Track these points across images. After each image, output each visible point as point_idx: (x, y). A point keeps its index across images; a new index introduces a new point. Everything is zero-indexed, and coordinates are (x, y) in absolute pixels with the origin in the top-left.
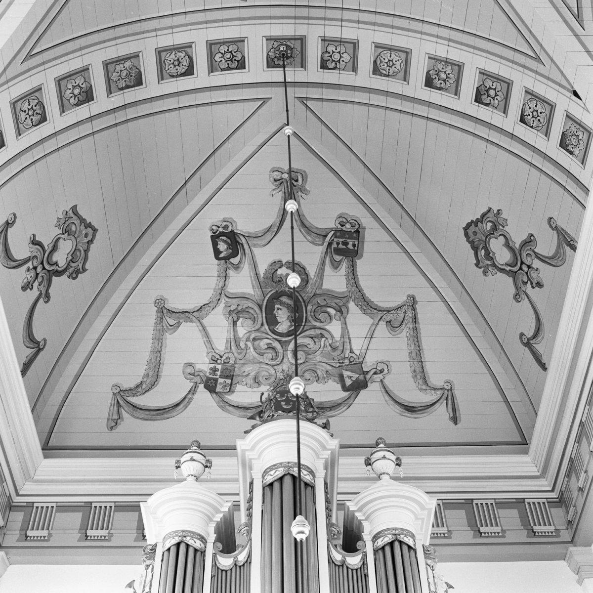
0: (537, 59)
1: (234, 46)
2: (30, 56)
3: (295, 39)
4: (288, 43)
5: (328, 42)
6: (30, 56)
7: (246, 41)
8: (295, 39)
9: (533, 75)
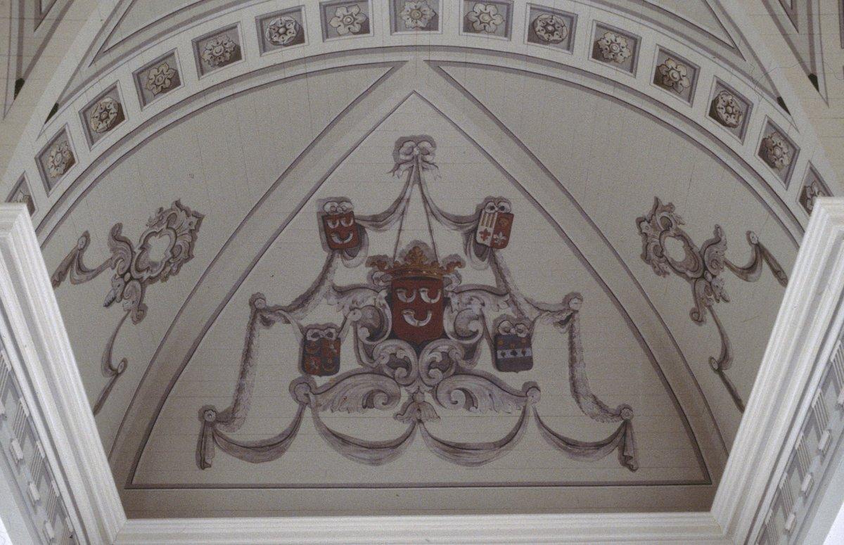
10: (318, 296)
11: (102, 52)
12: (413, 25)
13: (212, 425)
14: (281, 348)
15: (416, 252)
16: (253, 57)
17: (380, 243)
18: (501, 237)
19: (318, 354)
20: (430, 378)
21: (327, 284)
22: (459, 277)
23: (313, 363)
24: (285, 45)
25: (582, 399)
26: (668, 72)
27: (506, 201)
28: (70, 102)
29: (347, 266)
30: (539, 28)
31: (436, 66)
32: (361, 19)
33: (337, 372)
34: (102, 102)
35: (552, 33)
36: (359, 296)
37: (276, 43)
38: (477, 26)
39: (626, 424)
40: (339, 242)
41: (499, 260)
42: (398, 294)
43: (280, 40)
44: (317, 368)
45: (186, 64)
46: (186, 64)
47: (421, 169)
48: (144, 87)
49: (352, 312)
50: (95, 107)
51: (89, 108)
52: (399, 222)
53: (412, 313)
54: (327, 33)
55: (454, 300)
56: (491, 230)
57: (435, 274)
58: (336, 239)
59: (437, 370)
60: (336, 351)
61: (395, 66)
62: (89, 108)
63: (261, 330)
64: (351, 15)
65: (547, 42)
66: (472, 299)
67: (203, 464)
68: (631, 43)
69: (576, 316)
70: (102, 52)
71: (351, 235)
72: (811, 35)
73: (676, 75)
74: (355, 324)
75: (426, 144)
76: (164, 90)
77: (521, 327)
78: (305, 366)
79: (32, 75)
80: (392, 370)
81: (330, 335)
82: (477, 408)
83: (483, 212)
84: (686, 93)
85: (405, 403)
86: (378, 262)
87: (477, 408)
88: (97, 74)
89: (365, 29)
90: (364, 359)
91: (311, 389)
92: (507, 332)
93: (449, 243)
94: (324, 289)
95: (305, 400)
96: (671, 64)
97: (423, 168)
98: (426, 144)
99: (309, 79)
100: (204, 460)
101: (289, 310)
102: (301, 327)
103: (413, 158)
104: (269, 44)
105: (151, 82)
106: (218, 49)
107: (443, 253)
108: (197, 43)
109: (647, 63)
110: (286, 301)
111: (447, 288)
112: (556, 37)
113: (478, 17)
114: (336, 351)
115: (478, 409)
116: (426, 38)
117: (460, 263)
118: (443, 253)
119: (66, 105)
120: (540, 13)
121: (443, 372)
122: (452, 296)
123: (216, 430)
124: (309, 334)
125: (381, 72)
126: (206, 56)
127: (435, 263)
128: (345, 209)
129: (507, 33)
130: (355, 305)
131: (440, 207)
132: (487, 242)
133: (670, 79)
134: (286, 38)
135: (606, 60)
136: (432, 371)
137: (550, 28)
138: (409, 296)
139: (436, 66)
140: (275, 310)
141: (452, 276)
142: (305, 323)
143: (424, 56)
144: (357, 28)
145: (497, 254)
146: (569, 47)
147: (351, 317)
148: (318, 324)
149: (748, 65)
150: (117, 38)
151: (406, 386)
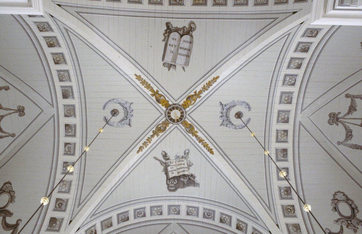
0: (78, 13)
1: (197, 3)
2: (275, 19)
3: (173, 4)
4: (175, 2)
5: (160, 3)
6: (275, 19)
7: (192, 4)
8: (173, 4)
9: (78, 6)
11: (94, 215)
12: (174, 213)
16: (132, 220)
24: (141, 217)
26: (239, 225)
28: (83, 227)
30: (206, 214)
31: (179, 224)
32: (160, 211)
34: (91, 229)
35: (209, 216)
37: (138, 217)
38: (190, 213)
43: (139, 216)
45: (115, 221)
46: (115, 221)
48: (103, 225)
50: (89, 230)
51: (88, 230)
54: (151, 214)
61: (169, 224)
62: (88, 230)
64: (158, 210)
65: (208, 218)
68: (229, 218)
70: (94, 215)
72: (275, 214)
73: (242, 226)
76: (108, 227)
79: (75, 219)
84: (245, 231)
88: (91, 221)
89: (161, 214)
96: (240, 223)
99: (146, 227)
104: (136, 217)
105: (105, 225)
106: (123, 217)
108: (118, 215)
109: (234, 223)
112: (210, 217)
113: (190, 211)
116: (176, 217)
119: (82, 228)
120: (205, 210)
125: (165, 226)
126: (120, 219)
129: (198, 216)
133: (240, 228)
134: (141, 215)
135: (223, 223)
137: (209, 214)
139: (179, 224)
143: (176, 222)
144: (159, 213)
146: (214, 219)
149: (260, 222)
150: (97, 212)
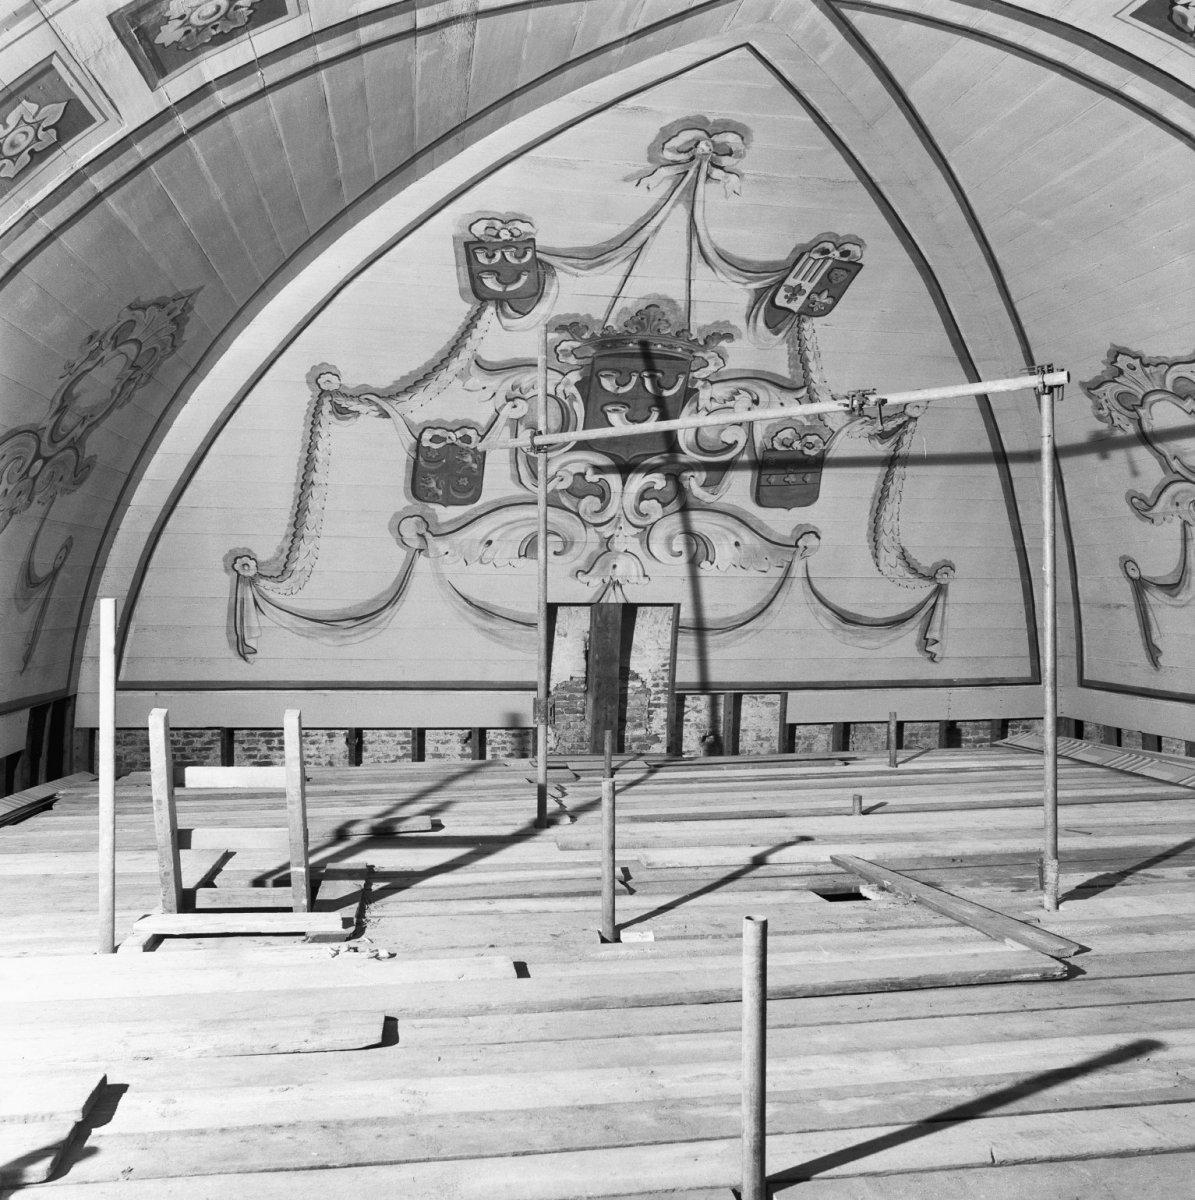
10: (445, 375)
13: (252, 581)
14: (370, 459)
15: (647, 315)
17: (578, 294)
18: (824, 298)
19: (443, 472)
20: (641, 514)
21: (465, 355)
22: (721, 356)
23: (433, 485)
25: (882, 553)
27: (859, 243)
29: (506, 329)
33: (475, 499)
36: (525, 379)
39: (940, 590)
40: (499, 288)
41: (807, 334)
42: (603, 379)
44: (440, 492)
47: (702, 177)
49: (511, 404)
52: (628, 263)
53: (625, 410)
55: (704, 395)
56: (808, 287)
57: (680, 350)
58: (491, 283)
59: (655, 501)
60: (475, 466)
63: (334, 431)
66: (738, 393)
67: (243, 650)
69: (911, 426)
71: (524, 278)
74: (515, 425)
75: (731, 139)
77: (812, 439)
78: (417, 488)
80: (575, 500)
81: (467, 439)
82: (712, 563)
83: (806, 257)
85: (592, 554)
86: (571, 326)
87: (712, 563)
90: (526, 481)
91: (428, 526)
92: (787, 447)
93: (722, 299)
94: (456, 364)
95: (416, 544)
97: (708, 176)
98: (731, 139)
100: (244, 640)
101: (392, 394)
102: (409, 426)
103: (692, 159)
107: (701, 320)
110: (383, 380)
111: (696, 374)
114: (475, 466)
115: (715, 564)
117: (729, 337)
118: (701, 320)
121: (664, 505)
122: (703, 387)
123: (258, 591)
124: (427, 435)
127: (683, 332)
128: (516, 233)
130: (517, 392)
131: (714, 239)
132: (795, 306)
136: (644, 503)
138: (619, 384)
140: (364, 394)
141: (708, 355)
142: (418, 418)
145: (805, 326)
147: (508, 412)
148: (442, 421)
151: (596, 525)
